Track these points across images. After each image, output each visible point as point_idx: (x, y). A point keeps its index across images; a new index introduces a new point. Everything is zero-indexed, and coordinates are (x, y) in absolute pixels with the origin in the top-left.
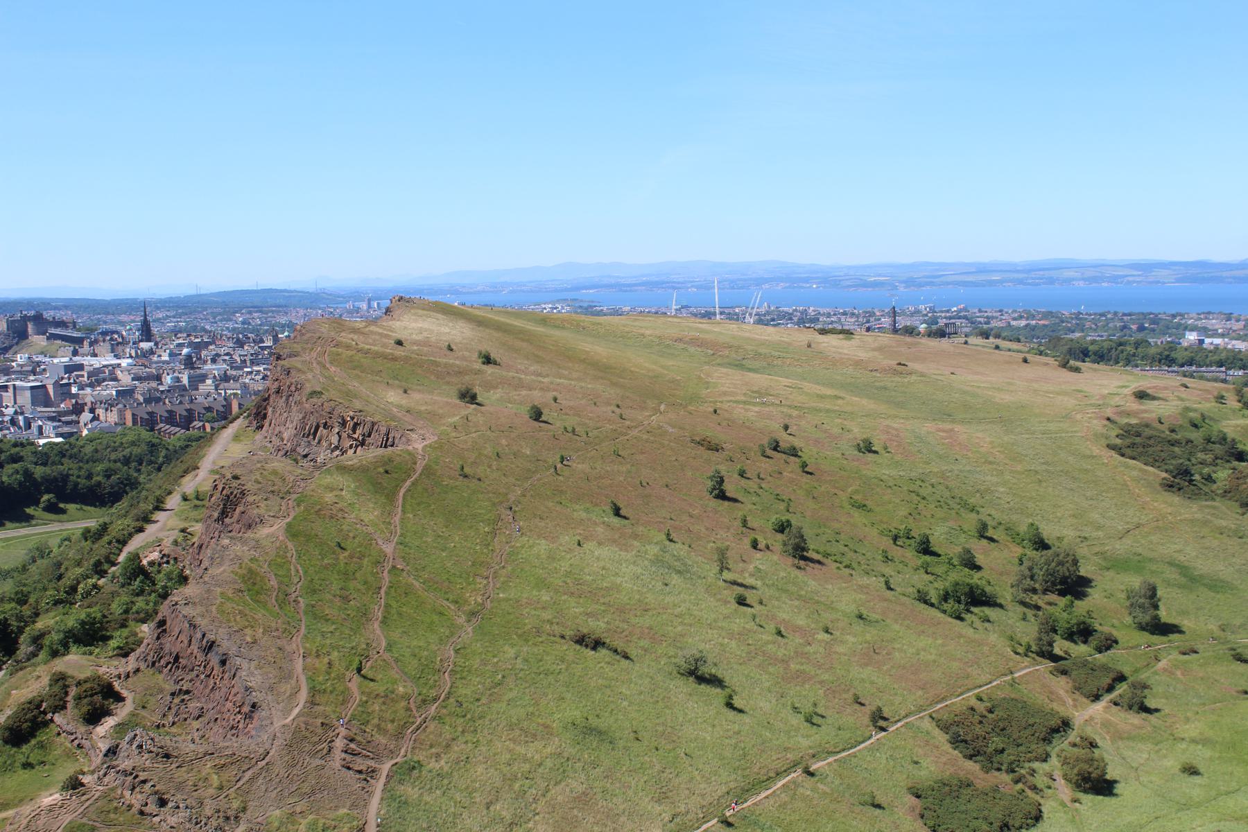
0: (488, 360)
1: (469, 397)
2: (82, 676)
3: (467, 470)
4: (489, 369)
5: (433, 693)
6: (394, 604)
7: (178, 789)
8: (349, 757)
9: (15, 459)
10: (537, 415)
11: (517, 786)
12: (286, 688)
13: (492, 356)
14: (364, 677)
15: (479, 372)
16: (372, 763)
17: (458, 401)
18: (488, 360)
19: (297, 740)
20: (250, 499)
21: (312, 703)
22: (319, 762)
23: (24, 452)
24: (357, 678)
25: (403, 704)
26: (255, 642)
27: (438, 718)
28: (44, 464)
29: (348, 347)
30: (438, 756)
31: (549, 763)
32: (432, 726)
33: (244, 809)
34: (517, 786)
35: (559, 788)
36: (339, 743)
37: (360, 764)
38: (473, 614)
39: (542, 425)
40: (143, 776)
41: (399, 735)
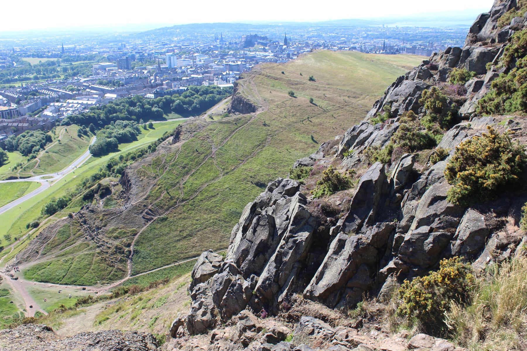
0: (311, 79)
1: (292, 94)
2: (105, 184)
3: (267, 122)
4: (311, 83)
5: (188, 198)
6: (201, 169)
7: (91, 219)
8: (146, 215)
9: (212, 92)
10: (311, 101)
11: (195, 227)
12: (142, 194)
13: (314, 78)
14: (168, 193)
15: (304, 84)
16: (152, 217)
17: (287, 95)
18: (311, 79)
19: (135, 208)
20: (181, 133)
21: (146, 199)
22: (136, 215)
23: (215, 90)
24: (166, 192)
25: (175, 200)
26: (142, 181)
27: (184, 206)
28: (220, 95)
29: (263, 75)
30: (175, 216)
31: (211, 221)
32: (180, 207)
33: (105, 226)
34: (195, 227)
35: (209, 228)
36: (146, 210)
37: (149, 217)
38: (227, 173)
39: (311, 104)
40: (84, 215)
41: (167, 209)
